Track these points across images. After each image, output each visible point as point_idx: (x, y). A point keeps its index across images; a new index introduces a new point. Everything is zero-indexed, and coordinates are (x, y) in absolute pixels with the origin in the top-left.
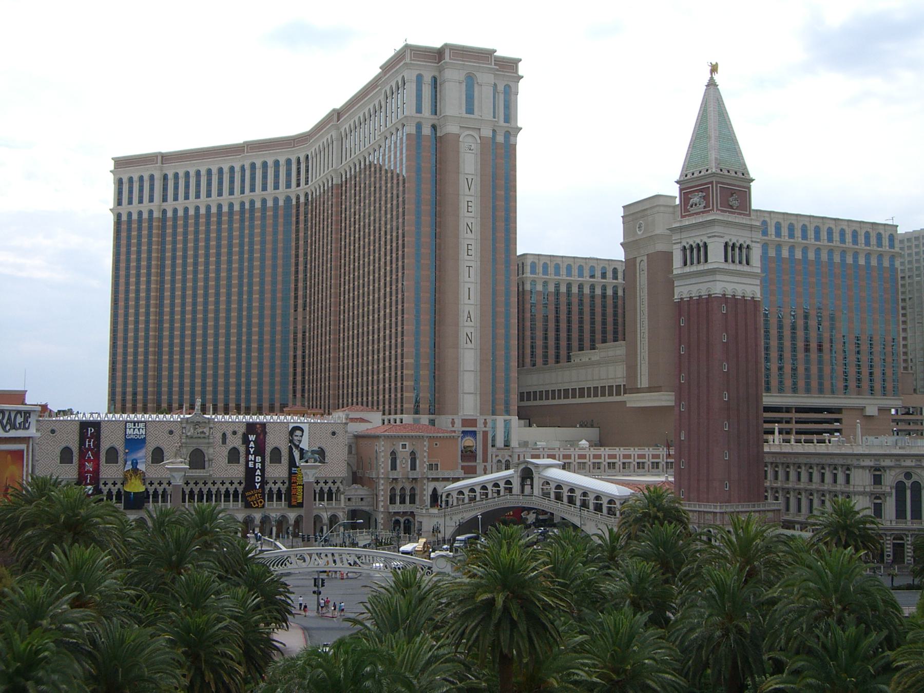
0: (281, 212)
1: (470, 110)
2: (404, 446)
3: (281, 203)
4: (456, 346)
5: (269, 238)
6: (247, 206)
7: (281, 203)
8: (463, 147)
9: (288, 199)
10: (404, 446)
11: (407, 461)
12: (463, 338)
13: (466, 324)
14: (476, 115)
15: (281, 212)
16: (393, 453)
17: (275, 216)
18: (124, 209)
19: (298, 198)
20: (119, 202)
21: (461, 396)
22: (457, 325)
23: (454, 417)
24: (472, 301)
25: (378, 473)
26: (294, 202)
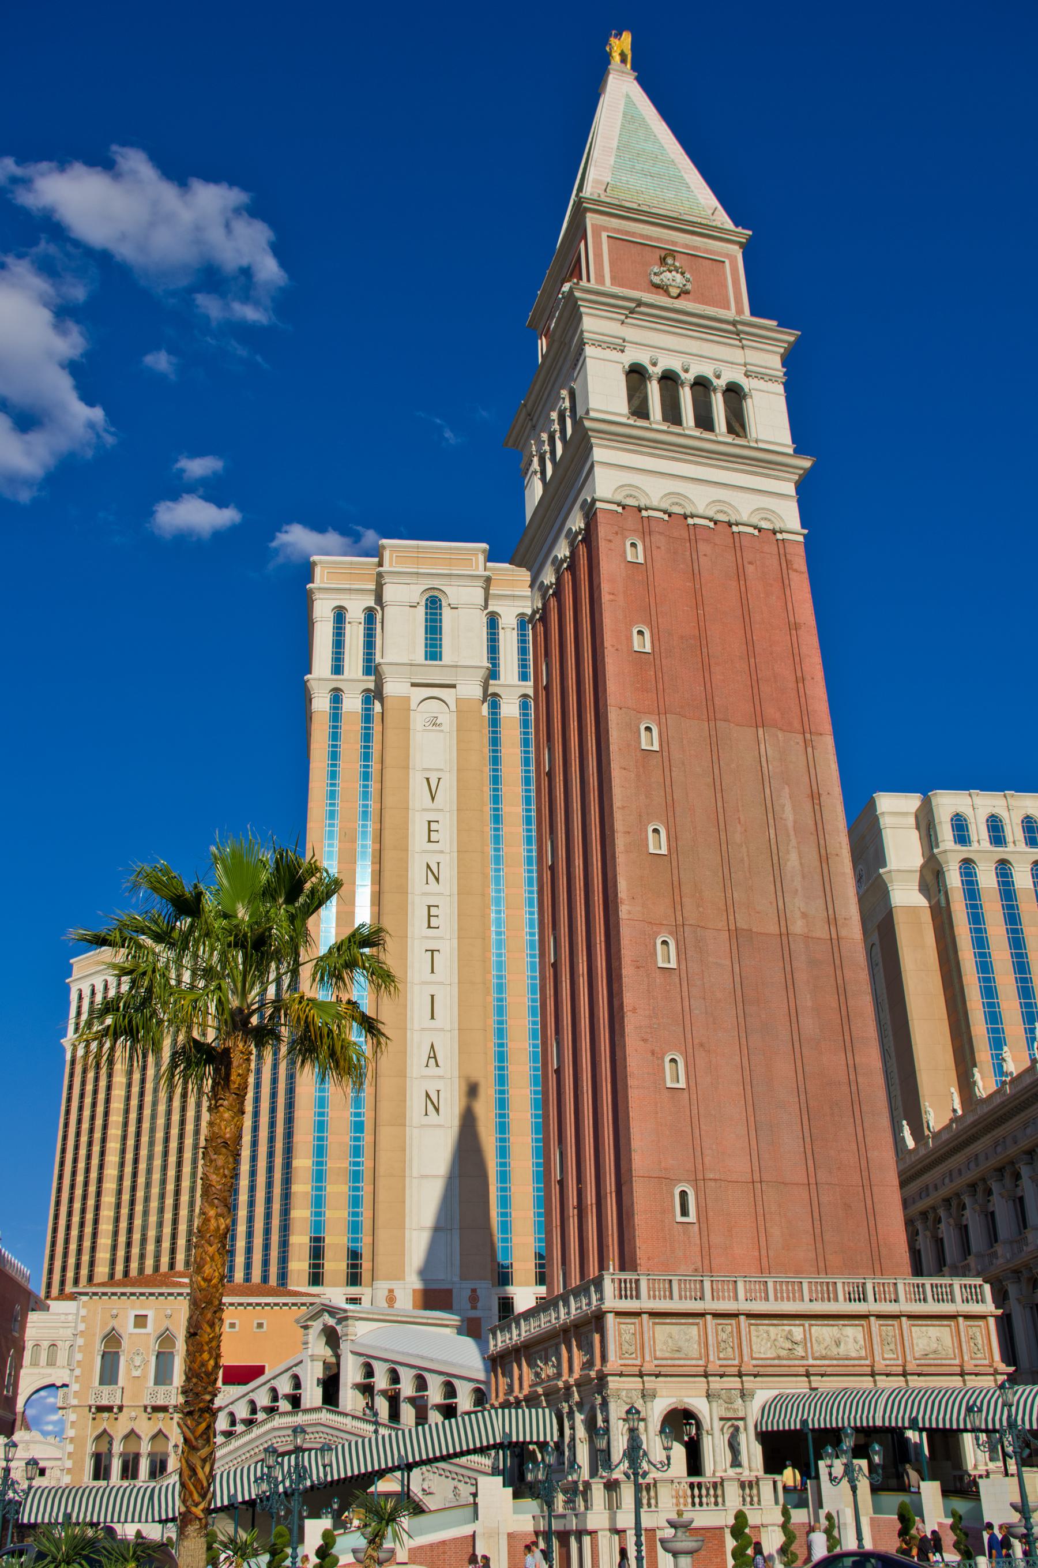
1: (433, 652)
2: (141, 1321)
4: (400, 1120)
8: (418, 720)
10: (141, 1321)
11: (146, 1363)
12: (416, 1103)
14: (447, 657)
16: (112, 1339)
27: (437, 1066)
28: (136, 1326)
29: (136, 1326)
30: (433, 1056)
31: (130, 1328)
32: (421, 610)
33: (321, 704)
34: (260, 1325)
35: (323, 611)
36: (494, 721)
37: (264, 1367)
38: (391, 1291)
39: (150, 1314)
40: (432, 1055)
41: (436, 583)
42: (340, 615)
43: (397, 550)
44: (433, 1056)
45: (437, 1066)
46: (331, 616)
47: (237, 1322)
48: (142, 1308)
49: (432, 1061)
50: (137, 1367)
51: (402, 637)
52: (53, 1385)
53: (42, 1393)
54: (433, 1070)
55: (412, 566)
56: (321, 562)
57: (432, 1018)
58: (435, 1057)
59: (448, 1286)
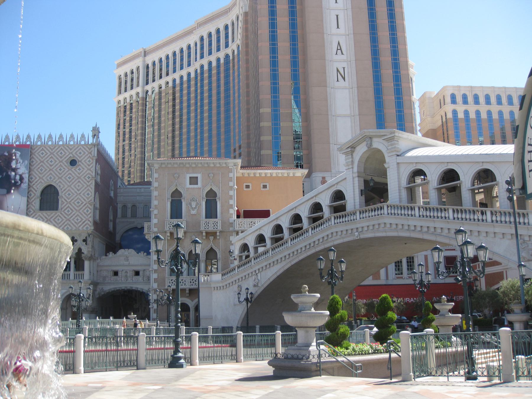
0: (222, 69)
2: (194, 181)
3: (222, 61)
4: (323, 84)
6: (199, 71)
7: (222, 61)
9: (227, 56)
10: (194, 181)
11: (198, 205)
12: (332, 75)
13: (335, 57)
15: (222, 69)
17: (218, 73)
18: (121, 97)
20: (120, 92)
22: (323, 58)
24: (342, 30)
26: (231, 58)
27: (342, 54)
30: (339, 48)
31: (188, 185)
34: (265, 187)
37: (269, 211)
39: (199, 176)
40: (339, 48)
44: (339, 48)
45: (342, 54)
47: (245, 189)
49: (339, 51)
50: (193, 209)
52: (136, 228)
53: (130, 233)
54: (340, 57)
57: (338, 27)
58: (341, 49)
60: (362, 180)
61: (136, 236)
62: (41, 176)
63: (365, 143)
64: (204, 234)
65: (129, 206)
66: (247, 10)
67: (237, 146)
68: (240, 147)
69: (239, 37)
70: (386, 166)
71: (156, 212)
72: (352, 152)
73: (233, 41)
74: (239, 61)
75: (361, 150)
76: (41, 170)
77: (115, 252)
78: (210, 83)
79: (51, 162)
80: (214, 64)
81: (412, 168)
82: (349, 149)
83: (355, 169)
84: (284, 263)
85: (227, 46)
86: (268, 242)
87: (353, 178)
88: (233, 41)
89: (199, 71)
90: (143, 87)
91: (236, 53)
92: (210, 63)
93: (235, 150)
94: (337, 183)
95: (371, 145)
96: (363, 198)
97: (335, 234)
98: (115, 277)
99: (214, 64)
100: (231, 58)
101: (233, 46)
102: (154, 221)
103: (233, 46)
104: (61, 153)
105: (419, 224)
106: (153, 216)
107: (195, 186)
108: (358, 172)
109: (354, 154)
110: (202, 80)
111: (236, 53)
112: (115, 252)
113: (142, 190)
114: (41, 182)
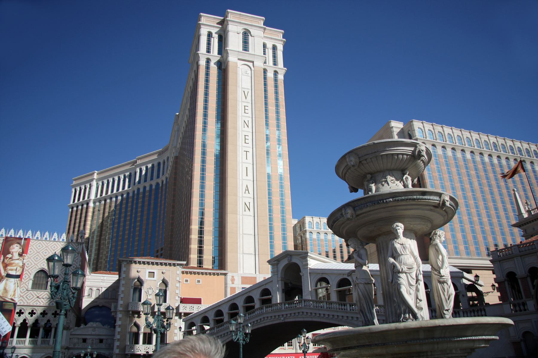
0: (153, 192)
2: (152, 274)
3: (154, 187)
4: (236, 212)
5: (146, 208)
6: (136, 192)
7: (154, 187)
8: (240, 72)
9: (158, 184)
10: (152, 274)
12: (241, 207)
13: (244, 195)
14: (251, 51)
15: (153, 192)
17: (150, 196)
19: (163, 182)
21: (240, 256)
22: (236, 195)
23: (234, 274)
25: (116, 307)
26: (160, 186)
28: (149, 277)
29: (149, 277)
31: (147, 278)
32: (241, 36)
33: (202, 63)
34: (199, 281)
35: (204, 32)
36: (265, 78)
38: (233, 277)
41: (247, 27)
42: (210, 35)
43: (232, 15)
46: (206, 33)
48: (152, 269)
51: (234, 42)
53: (93, 309)
54: (247, 195)
55: (238, 22)
56: (203, 16)
59: (255, 276)
60: (283, 282)
61: (97, 312)
62: (36, 263)
63: (287, 259)
64: (131, 313)
65: (94, 289)
66: (177, 155)
67: (159, 248)
68: (162, 249)
69: (168, 172)
70: (301, 274)
71: (122, 296)
72: (277, 264)
73: (163, 174)
74: (166, 188)
75: (284, 262)
76: (37, 258)
77: (86, 324)
78: (143, 202)
79: (46, 253)
80: (148, 189)
81: (319, 277)
82: (276, 262)
83: (279, 276)
84: (226, 338)
85: (158, 177)
86: (212, 322)
87: (278, 281)
88: (163, 174)
89: (136, 192)
90: (437, 269)
91: (164, 182)
92: (145, 188)
93: (157, 251)
94: (266, 284)
95: (291, 260)
96: (284, 294)
97: (266, 318)
98: (84, 343)
99: (148, 189)
100: (160, 186)
101: (163, 178)
102: (121, 302)
103: (163, 178)
104: (54, 247)
105: (327, 313)
106: (120, 299)
107: (152, 279)
108: (281, 278)
109: (279, 265)
110: (138, 199)
111: (164, 182)
112: (86, 324)
113: (105, 278)
114: (35, 267)
